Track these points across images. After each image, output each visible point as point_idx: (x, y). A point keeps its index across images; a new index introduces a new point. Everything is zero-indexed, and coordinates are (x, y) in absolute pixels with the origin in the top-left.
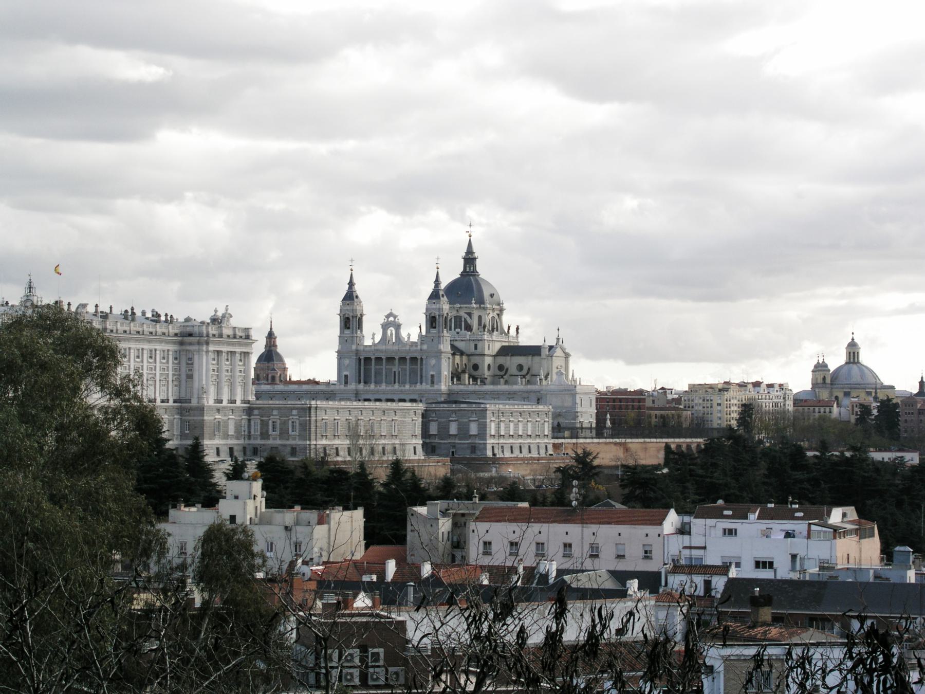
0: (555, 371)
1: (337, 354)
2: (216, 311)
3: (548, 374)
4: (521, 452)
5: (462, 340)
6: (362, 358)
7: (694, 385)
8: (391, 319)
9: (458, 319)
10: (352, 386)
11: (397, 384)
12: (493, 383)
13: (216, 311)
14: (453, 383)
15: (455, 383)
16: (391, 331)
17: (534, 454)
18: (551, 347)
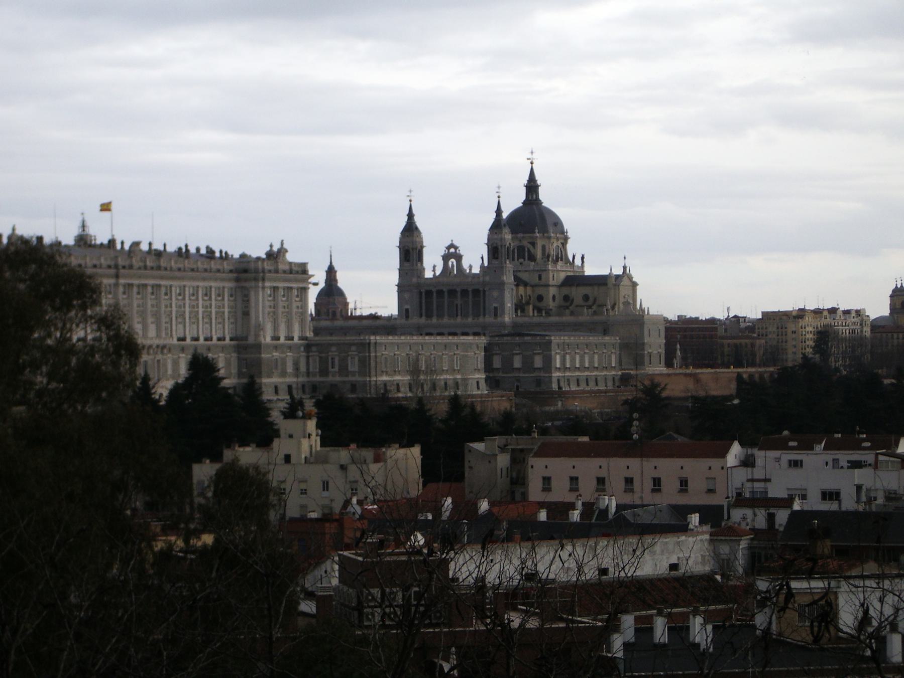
0: (622, 300)
1: (397, 287)
2: (271, 246)
3: (615, 304)
4: (588, 385)
5: (526, 271)
6: (423, 290)
7: (767, 313)
8: (452, 250)
9: (521, 249)
10: (415, 320)
11: (459, 317)
12: (560, 315)
13: (271, 246)
14: (517, 315)
15: (519, 315)
16: (452, 263)
17: (602, 387)
18: (617, 277)
